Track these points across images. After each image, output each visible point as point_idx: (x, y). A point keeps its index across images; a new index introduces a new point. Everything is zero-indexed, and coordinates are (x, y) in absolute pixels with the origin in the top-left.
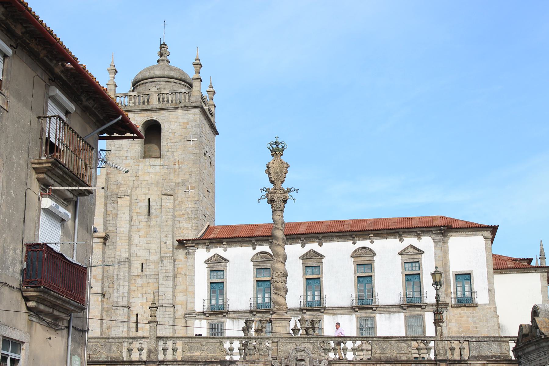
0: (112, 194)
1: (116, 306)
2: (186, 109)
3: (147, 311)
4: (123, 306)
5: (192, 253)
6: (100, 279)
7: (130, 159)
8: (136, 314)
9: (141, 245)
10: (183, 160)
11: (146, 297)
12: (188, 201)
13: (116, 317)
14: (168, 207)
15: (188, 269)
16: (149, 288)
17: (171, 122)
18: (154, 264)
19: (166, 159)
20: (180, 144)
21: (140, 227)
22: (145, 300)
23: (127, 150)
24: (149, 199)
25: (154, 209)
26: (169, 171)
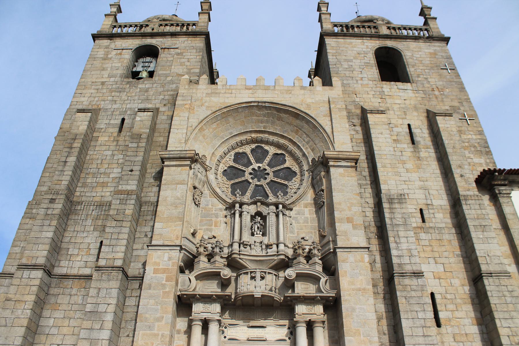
0: (350, 115)
1: (400, 272)
2: (429, 41)
3: (449, 287)
4: (414, 273)
5: (505, 195)
6: (361, 225)
7: (367, 80)
8: (430, 293)
9: (412, 183)
10: (444, 87)
11: (443, 264)
12: (468, 130)
13: (405, 293)
14: (449, 129)
15: (509, 219)
16: (443, 249)
17: (413, 51)
18: (441, 211)
19: (418, 84)
20: (433, 71)
21: (404, 158)
22: (441, 268)
23: (361, 72)
24: (409, 125)
25: (421, 138)
26: (428, 97)
